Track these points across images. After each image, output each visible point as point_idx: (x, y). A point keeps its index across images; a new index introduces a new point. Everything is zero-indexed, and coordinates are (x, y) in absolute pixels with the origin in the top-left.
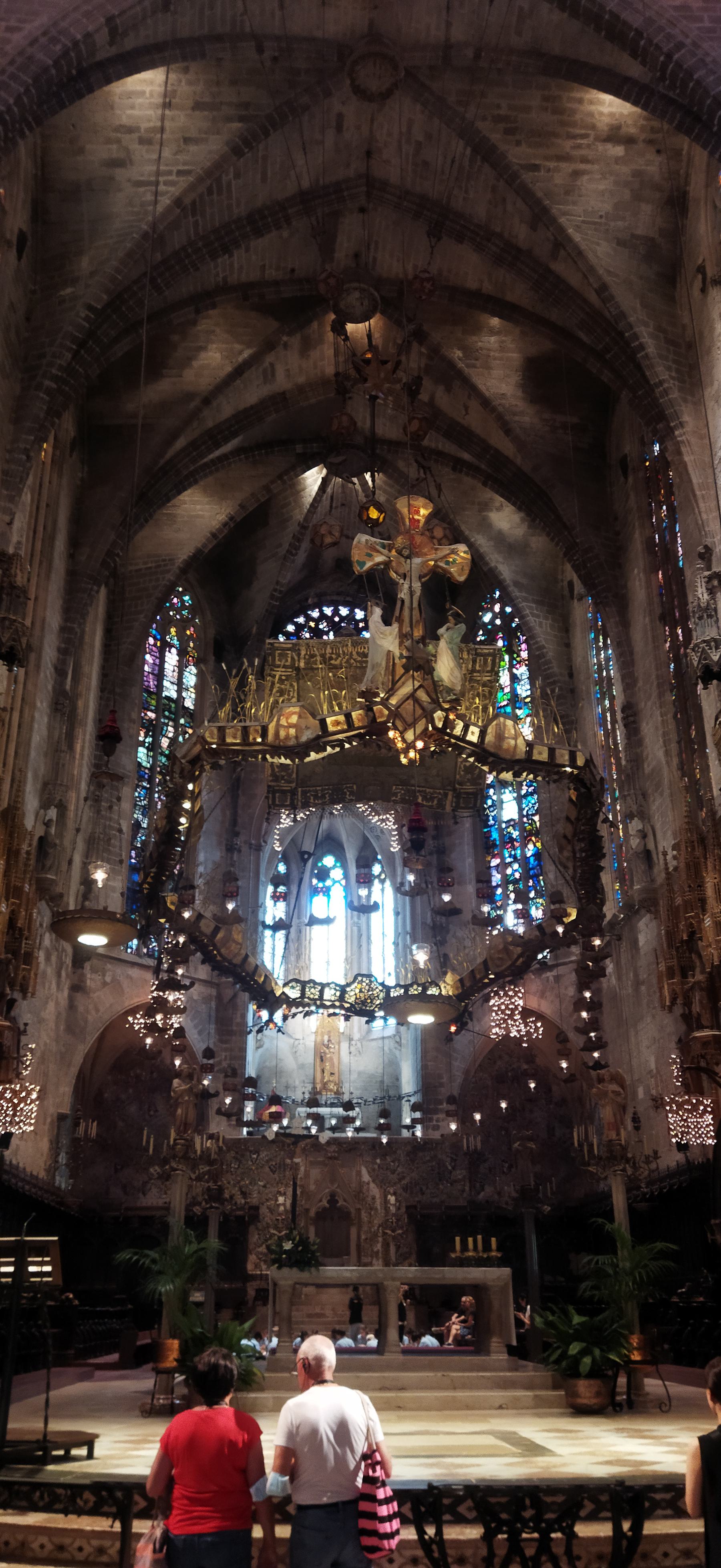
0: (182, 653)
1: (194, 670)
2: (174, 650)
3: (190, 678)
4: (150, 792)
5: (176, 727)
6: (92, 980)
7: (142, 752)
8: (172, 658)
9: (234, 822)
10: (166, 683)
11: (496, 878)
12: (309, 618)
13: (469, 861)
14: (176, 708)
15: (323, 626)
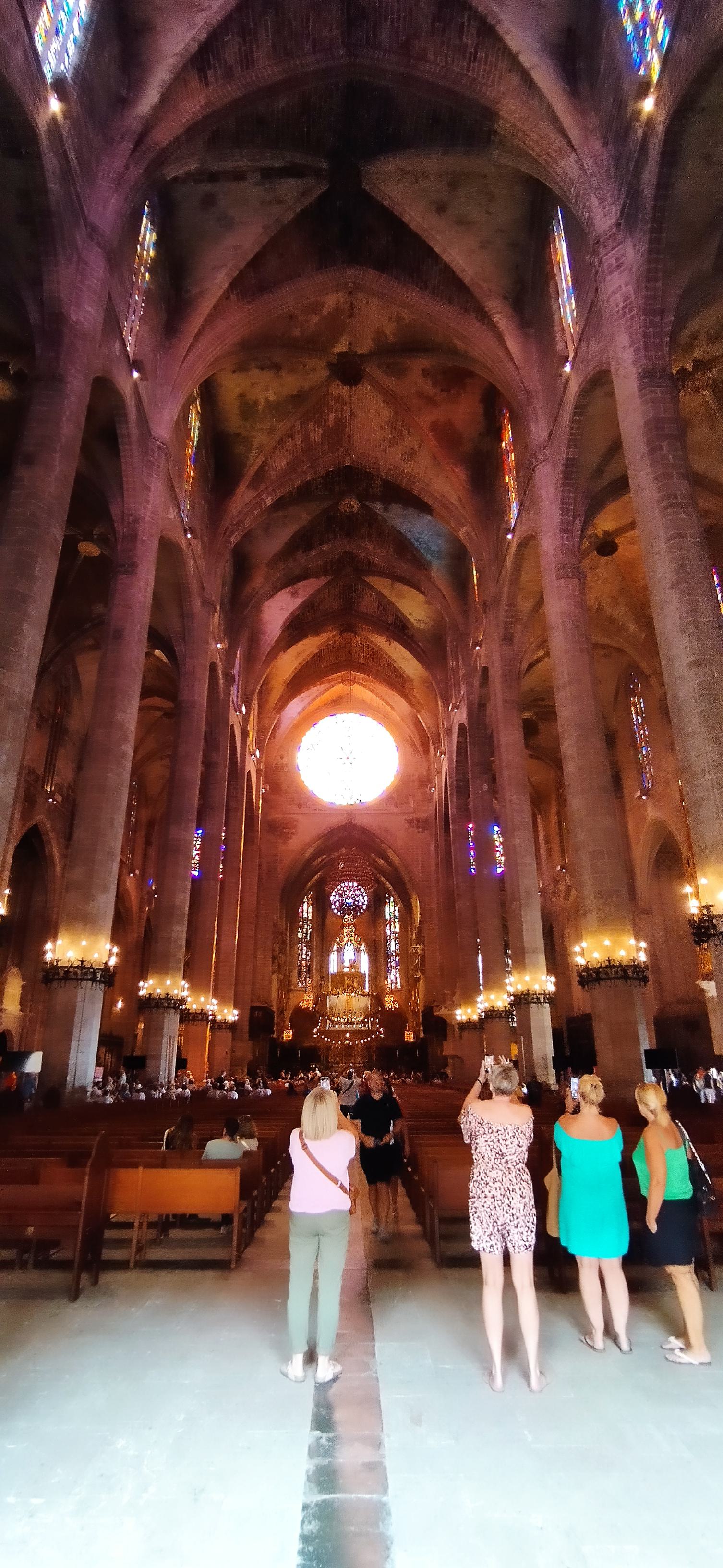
0: (308, 903)
1: (311, 907)
2: (306, 903)
3: (310, 910)
4: (302, 945)
5: (308, 925)
6: (291, 995)
7: (299, 934)
8: (305, 905)
9: (322, 948)
10: (304, 913)
11: (389, 965)
12: (341, 887)
13: (383, 960)
14: (308, 919)
15: (345, 889)
